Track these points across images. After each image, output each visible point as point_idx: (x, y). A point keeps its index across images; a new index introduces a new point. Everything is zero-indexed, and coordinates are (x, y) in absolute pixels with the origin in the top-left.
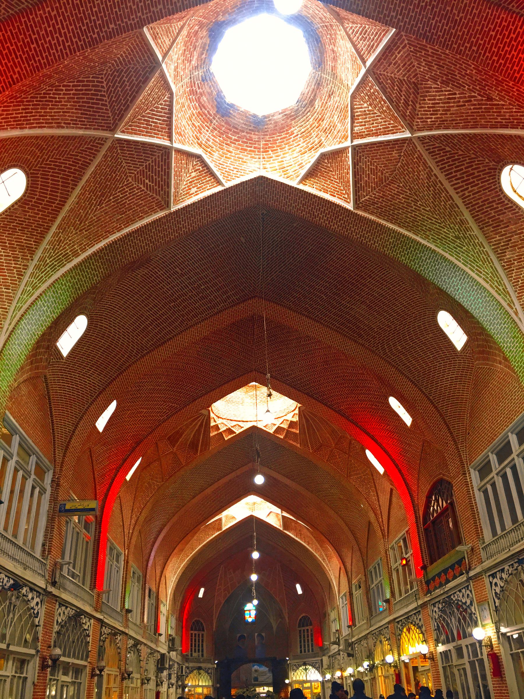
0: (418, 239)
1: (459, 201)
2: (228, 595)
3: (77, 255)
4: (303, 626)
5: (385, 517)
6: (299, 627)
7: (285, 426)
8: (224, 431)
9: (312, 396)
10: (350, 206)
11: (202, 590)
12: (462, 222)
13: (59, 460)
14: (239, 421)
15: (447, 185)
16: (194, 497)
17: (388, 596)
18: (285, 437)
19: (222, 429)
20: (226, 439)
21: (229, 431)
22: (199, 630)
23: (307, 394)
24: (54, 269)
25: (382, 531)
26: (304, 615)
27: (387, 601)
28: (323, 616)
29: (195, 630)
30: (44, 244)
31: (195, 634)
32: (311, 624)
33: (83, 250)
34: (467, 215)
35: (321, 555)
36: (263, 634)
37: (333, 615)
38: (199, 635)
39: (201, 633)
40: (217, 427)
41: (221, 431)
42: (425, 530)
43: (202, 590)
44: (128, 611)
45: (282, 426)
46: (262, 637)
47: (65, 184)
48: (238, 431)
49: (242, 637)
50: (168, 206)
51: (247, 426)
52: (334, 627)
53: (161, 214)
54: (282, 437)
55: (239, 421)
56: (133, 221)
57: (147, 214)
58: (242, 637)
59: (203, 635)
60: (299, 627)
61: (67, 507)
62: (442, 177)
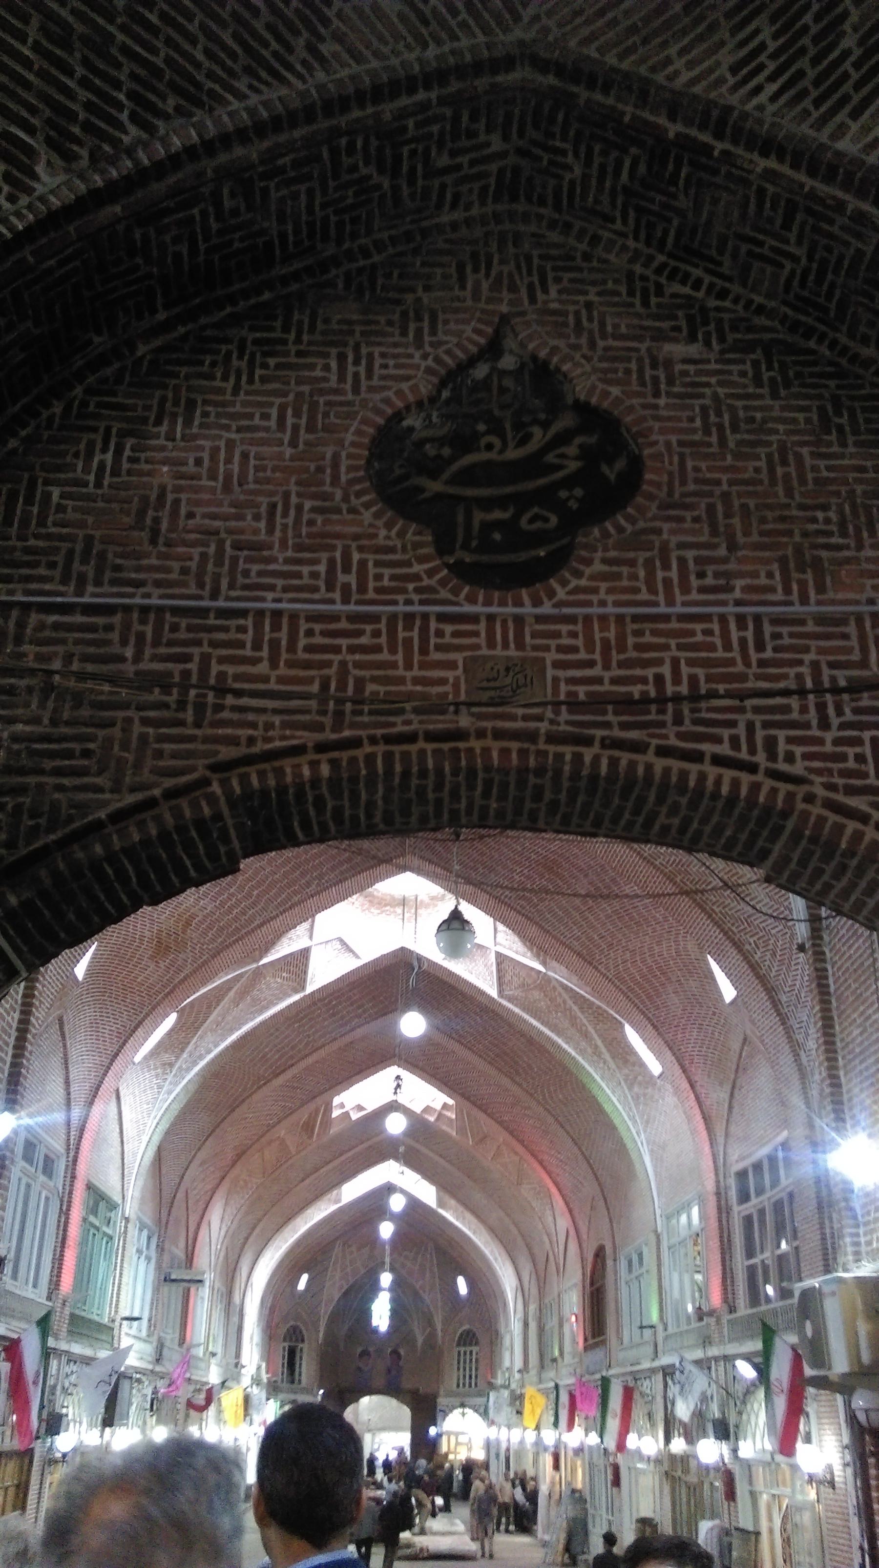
0: (560, 1041)
1: (592, 1031)
2: (346, 1287)
3: (209, 1052)
4: (465, 1345)
5: (562, 1247)
6: (459, 1345)
7: (438, 1106)
9: (468, 1099)
10: (493, 993)
11: (305, 1278)
12: (596, 1047)
13: (164, 1221)
15: (579, 1014)
16: (303, 1180)
17: (556, 1353)
18: (438, 1119)
23: (463, 1095)
24: (188, 1070)
25: (557, 1265)
26: (466, 1327)
27: (554, 1360)
28: (494, 1338)
30: (185, 1055)
32: (477, 1344)
33: (216, 1046)
34: (599, 1042)
35: (492, 1252)
36: (402, 1352)
37: (507, 1342)
40: (342, 1106)
42: (592, 1293)
43: (305, 1278)
44: (214, 1355)
45: (432, 1105)
46: (399, 1356)
47: (209, 1007)
49: (365, 1353)
50: (303, 988)
52: (507, 1363)
53: (296, 997)
54: (432, 1119)
56: (267, 1008)
57: (281, 999)
58: (365, 1353)
60: (459, 1345)
61: (173, 1277)
62: (575, 1008)
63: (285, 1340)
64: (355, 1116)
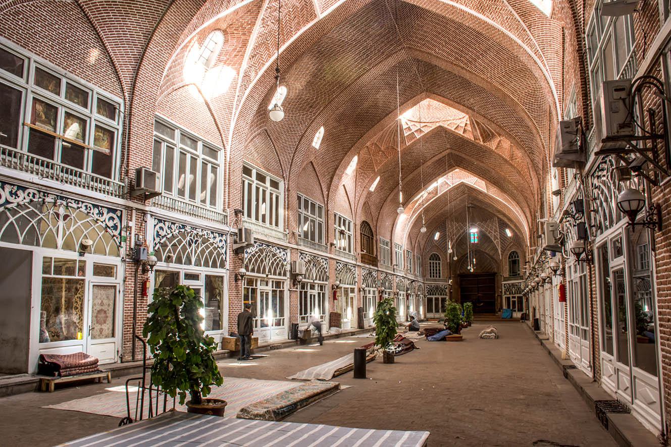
8: (416, 131)
14: (428, 123)
19: (414, 129)
20: (418, 137)
21: (419, 131)
22: (436, 260)
29: (433, 260)
31: (433, 263)
38: (436, 263)
39: (437, 262)
40: (409, 129)
41: (413, 131)
48: (426, 130)
51: (434, 126)
55: (428, 123)
59: (439, 264)
63: (430, 260)
64: (418, 136)
